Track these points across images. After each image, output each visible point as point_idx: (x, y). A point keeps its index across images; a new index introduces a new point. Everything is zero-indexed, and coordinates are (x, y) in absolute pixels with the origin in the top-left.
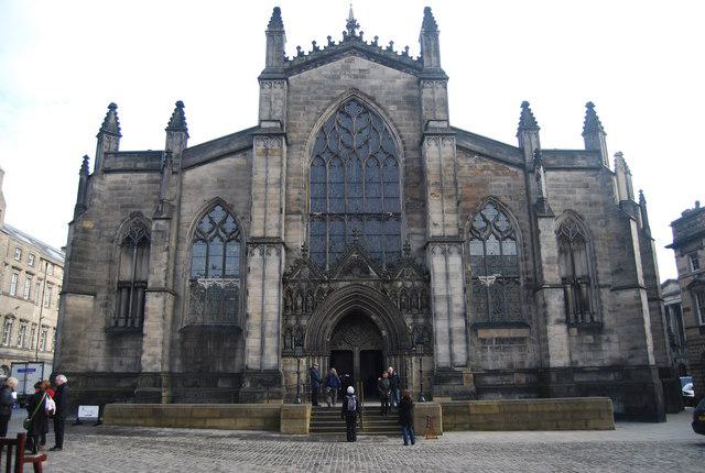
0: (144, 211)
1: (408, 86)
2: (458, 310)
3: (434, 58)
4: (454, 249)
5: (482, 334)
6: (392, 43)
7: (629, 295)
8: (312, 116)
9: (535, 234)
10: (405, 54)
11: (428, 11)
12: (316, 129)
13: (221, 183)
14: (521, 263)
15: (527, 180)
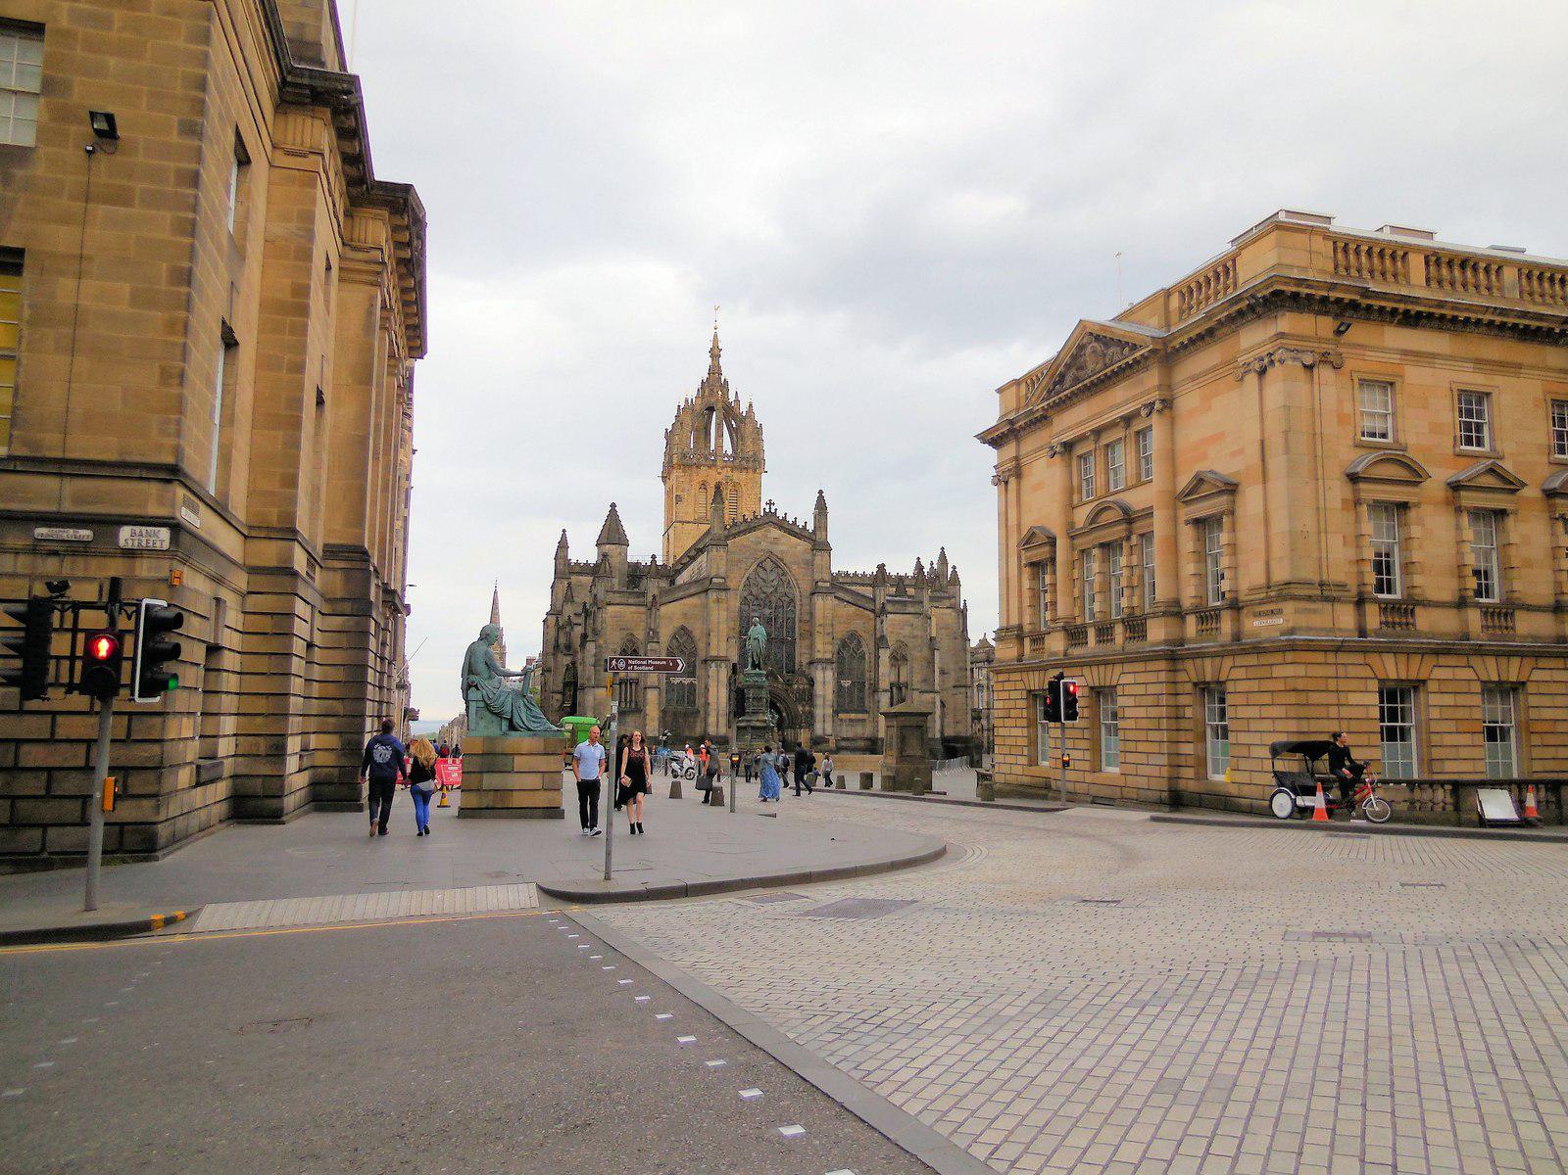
0: (635, 634)
2: (829, 703)
3: (823, 533)
4: (829, 667)
5: (841, 716)
6: (796, 518)
7: (928, 697)
8: (743, 571)
9: (877, 657)
10: (804, 527)
11: (821, 492)
14: (867, 675)
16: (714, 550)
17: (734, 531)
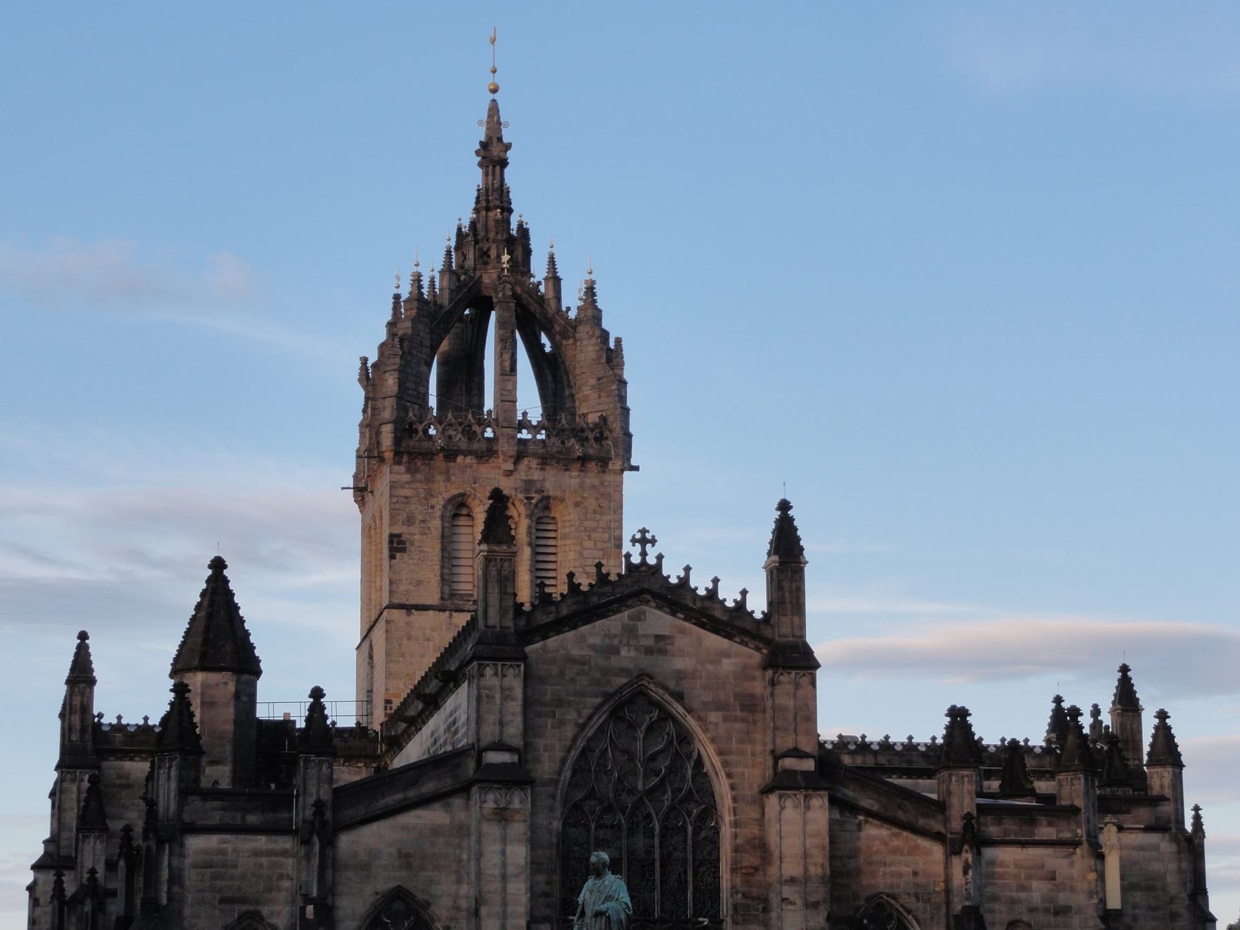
0: (265, 910)
1: (744, 674)
8: (569, 732)
10: (741, 605)
11: (784, 506)
12: (574, 754)
13: (406, 859)
15: (947, 865)
16: (489, 671)
17: (542, 619)
